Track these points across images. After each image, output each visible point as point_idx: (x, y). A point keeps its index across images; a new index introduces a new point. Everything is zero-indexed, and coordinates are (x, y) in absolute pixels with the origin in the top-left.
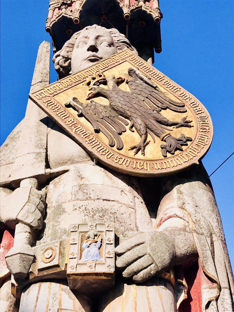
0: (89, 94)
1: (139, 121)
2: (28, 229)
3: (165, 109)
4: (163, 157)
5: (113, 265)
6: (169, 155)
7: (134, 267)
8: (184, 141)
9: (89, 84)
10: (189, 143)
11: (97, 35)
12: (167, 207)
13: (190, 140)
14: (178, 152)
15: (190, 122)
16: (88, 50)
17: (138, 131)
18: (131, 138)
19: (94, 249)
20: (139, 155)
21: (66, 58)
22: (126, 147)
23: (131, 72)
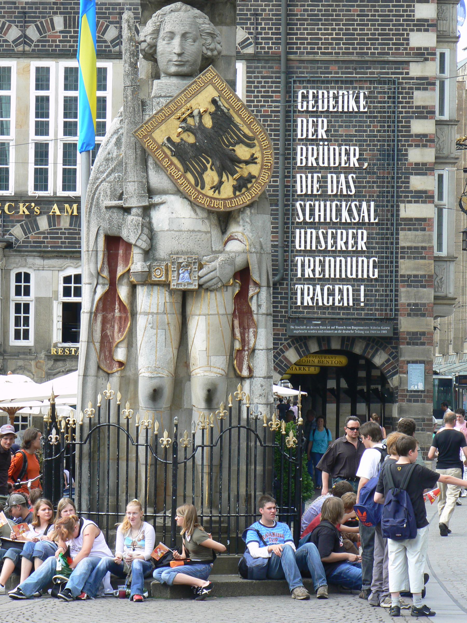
1: (218, 163)
3: (239, 143)
4: (232, 196)
5: (197, 284)
6: (238, 193)
7: (209, 284)
8: (251, 177)
9: (179, 118)
10: (254, 180)
11: (183, 32)
13: (254, 177)
15: (256, 158)
17: (218, 172)
18: (211, 176)
19: (187, 275)
20: (216, 195)
22: (207, 187)
23: (214, 102)
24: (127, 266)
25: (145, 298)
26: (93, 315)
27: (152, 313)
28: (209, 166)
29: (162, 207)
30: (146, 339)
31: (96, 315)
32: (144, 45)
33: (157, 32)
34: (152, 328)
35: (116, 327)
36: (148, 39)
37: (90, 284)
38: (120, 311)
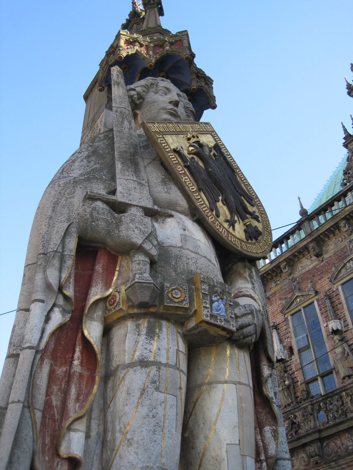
0: (192, 150)
2: (148, 260)
4: (245, 240)
6: (250, 241)
9: (189, 139)
12: (241, 286)
14: (254, 241)
16: (171, 102)
20: (231, 230)
21: (141, 96)
24: (107, 289)
25: (143, 337)
26: (39, 356)
27: (158, 364)
28: (220, 198)
29: (169, 220)
30: (144, 411)
31: (42, 359)
32: (132, 93)
33: (148, 88)
34: (157, 389)
35: (73, 391)
36: (138, 89)
37: (43, 301)
38: (82, 364)
